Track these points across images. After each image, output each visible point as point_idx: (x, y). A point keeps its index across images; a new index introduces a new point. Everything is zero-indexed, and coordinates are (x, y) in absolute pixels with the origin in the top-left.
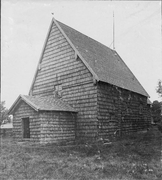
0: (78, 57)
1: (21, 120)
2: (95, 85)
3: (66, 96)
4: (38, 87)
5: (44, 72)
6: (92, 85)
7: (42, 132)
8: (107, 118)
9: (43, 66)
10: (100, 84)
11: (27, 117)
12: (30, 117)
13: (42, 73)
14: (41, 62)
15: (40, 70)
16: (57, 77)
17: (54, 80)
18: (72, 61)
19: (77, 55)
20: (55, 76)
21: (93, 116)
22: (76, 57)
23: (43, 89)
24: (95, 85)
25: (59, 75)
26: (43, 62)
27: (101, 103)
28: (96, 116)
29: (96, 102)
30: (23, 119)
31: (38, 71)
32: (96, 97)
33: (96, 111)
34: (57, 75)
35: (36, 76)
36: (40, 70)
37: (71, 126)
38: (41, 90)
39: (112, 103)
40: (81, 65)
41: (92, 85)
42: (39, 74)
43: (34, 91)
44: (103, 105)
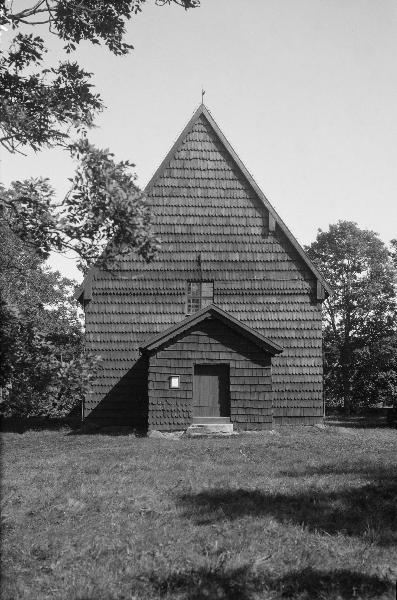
11: (218, 362)
12: (232, 365)
20: (193, 257)
22: (272, 226)
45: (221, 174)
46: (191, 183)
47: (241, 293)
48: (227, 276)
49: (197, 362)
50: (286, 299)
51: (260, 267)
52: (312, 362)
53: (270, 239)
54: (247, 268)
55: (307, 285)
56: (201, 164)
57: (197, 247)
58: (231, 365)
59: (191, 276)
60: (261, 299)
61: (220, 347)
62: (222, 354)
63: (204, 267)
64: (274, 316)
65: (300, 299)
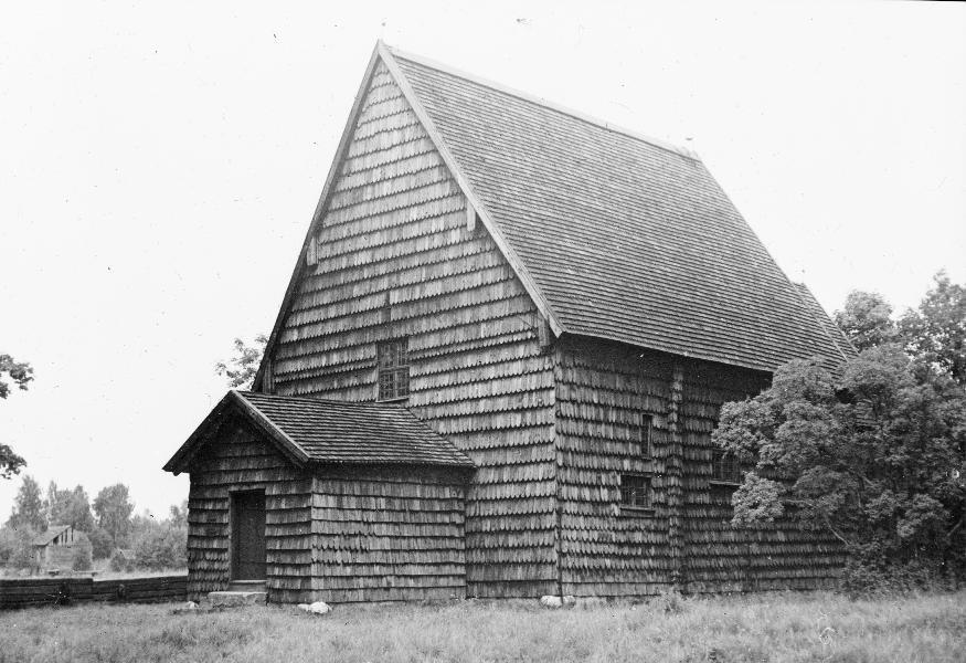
0: (479, 222)
1: (223, 500)
2: (546, 352)
4: (301, 351)
5: (328, 282)
6: (535, 350)
7: (315, 555)
8: (604, 494)
9: (326, 251)
10: (569, 346)
11: (255, 487)
15: (315, 267)
16: (387, 308)
17: (379, 318)
18: (455, 237)
19: (477, 215)
20: (379, 301)
21: (539, 490)
22: (471, 226)
24: (546, 352)
25: (395, 297)
26: (324, 237)
27: (580, 428)
28: (551, 488)
29: (552, 429)
30: (233, 494)
32: (553, 402)
33: (553, 467)
34: (388, 296)
36: (315, 267)
37: (447, 531)
38: (314, 363)
39: (633, 428)
40: (491, 260)
41: (535, 350)
44: (585, 437)
45: (410, 150)
46: (376, 175)
47: (445, 352)
48: (424, 326)
49: (233, 489)
50: (505, 354)
51: (464, 300)
52: (540, 472)
56: (385, 141)
57: (384, 284)
58: (267, 492)
59: (381, 336)
60: (470, 361)
63: (395, 315)
64: (480, 390)
65: (521, 351)
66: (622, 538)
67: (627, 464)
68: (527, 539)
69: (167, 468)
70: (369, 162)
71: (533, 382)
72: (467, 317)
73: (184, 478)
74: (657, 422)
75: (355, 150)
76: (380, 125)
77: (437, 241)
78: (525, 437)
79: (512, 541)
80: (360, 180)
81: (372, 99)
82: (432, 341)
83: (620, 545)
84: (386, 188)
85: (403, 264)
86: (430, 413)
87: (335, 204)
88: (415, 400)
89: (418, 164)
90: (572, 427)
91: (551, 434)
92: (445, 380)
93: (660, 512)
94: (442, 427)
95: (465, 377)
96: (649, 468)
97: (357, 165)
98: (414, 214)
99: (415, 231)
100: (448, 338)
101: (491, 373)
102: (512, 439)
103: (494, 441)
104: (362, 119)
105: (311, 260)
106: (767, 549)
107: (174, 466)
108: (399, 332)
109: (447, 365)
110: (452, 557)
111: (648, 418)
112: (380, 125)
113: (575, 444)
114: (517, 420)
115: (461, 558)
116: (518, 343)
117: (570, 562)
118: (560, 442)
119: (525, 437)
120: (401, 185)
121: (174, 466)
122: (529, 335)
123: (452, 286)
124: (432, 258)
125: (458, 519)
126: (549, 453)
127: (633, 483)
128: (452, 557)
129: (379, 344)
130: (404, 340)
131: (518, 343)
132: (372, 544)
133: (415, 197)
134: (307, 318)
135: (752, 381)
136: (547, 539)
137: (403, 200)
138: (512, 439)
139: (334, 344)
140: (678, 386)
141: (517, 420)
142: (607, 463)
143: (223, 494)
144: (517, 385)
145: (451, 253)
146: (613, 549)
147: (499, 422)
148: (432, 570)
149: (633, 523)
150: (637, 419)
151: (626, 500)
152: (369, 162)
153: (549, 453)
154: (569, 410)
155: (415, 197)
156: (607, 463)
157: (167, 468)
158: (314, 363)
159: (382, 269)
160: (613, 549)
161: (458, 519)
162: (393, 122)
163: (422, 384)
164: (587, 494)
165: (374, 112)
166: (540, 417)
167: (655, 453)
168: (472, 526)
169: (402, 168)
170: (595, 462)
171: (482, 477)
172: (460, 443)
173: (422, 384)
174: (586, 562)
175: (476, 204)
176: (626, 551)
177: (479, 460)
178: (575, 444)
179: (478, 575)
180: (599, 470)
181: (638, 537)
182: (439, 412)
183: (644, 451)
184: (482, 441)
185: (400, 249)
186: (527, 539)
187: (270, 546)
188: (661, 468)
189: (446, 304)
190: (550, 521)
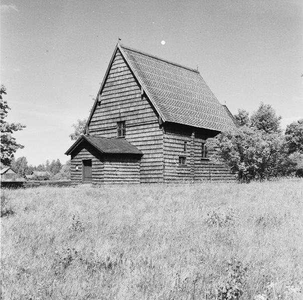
3: (130, 136)
4: (96, 123)
5: (104, 106)
7: (105, 176)
8: (175, 161)
9: (104, 98)
12: (93, 160)
13: (102, 106)
14: (101, 92)
17: (118, 116)
18: (138, 96)
20: (117, 111)
21: (159, 160)
22: (142, 93)
23: (103, 126)
26: (103, 94)
30: (83, 161)
31: (98, 103)
35: (95, 109)
38: (100, 126)
41: (158, 125)
42: (98, 107)
43: (90, 128)
48: (129, 118)
51: (140, 112)
52: (160, 155)
53: (144, 98)
54: (135, 113)
55: (157, 117)
56: (119, 70)
59: (119, 120)
60: (142, 127)
61: (88, 153)
62: (90, 156)
63: (122, 115)
65: (154, 125)
66: (179, 172)
67: (181, 154)
68: (156, 172)
69: (65, 154)
70: (115, 75)
71: (158, 133)
72: (141, 116)
73: (70, 156)
74: (188, 143)
75: (111, 72)
76: (118, 66)
77: (133, 97)
78: (155, 147)
79: (152, 172)
80: (113, 80)
81: (116, 59)
82: (131, 122)
83: (178, 173)
84: (119, 82)
85: (124, 102)
86: (131, 140)
87: (106, 86)
88: (127, 137)
89: (127, 77)
90: (167, 144)
91: (162, 146)
92: (135, 132)
93: (189, 165)
94: (134, 144)
95: (140, 131)
96: (185, 154)
97: (112, 76)
98: (127, 89)
99: (127, 93)
100: (136, 121)
101: (147, 130)
102: (152, 147)
103: (148, 147)
104: (113, 64)
105: (99, 100)
106: (214, 175)
107: (67, 154)
108: (123, 119)
109: (135, 128)
110: (137, 176)
111: (186, 142)
112: (118, 66)
113: (168, 149)
114: (153, 142)
115: (139, 177)
116: (154, 123)
117: (166, 178)
118: (164, 148)
119: (155, 147)
120: (123, 82)
121: (67, 154)
122: (157, 121)
123: (137, 108)
124: (132, 101)
125: (138, 167)
126: (161, 151)
127: (182, 158)
128: (137, 176)
129: (118, 122)
130: (124, 121)
131: (154, 123)
132: (118, 173)
133: (127, 85)
134: (100, 115)
135: (213, 134)
136: (161, 172)
137: (124, 86)
138: (152, 147)
139: (106, 122)
140: (193, 134)
141: (153, 142)
142: (175, 153)
143: (80, 160)
144: (153, 134)
145: (136, 100)
146: (177, 175)
147: (149, 143)
148: (132, 179)
149: (182, 168)
150: (183, 143)
151: (180, 163)
152: (115, 75)
153: (161, 151)
154: (166, 140)
155: (127, 85)
156: (175, 153)
157: (65, 154)
158: (100, 126)
159: (118, 103)
160: (177, 175)
161: (138, 167)
162: (121, 65)
163: (129, 133)
164: (171, 161)
165: (116, 62)
166: (160, 142)
167: (187, 151)
168: (142, 169)
169: (124, 77)
170: (173, 153)
171: (144, 156)
172: (139, 148)
173: (129, 133)
174: (170, 178)
175: (144, 87)
176: (180, 175)
177: (143, 152)
178: (168, 149)
179: (143, 181)
180: (174, 155)
181: (183, 172)
182: (134, 140)
183: (185, 150)
184: (144, 148)
185: (123, 98)
186: (156, 172)
187: (93, 173)
188: (189, 155)
189: (135, 113)
190: (161, 168)
